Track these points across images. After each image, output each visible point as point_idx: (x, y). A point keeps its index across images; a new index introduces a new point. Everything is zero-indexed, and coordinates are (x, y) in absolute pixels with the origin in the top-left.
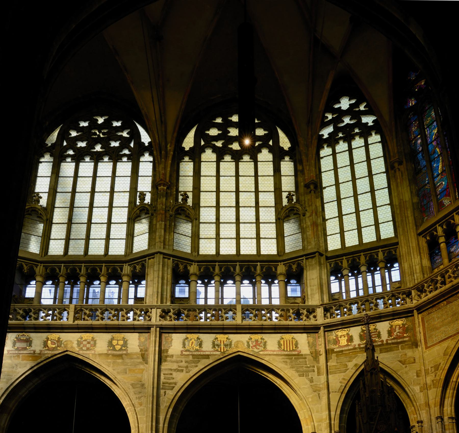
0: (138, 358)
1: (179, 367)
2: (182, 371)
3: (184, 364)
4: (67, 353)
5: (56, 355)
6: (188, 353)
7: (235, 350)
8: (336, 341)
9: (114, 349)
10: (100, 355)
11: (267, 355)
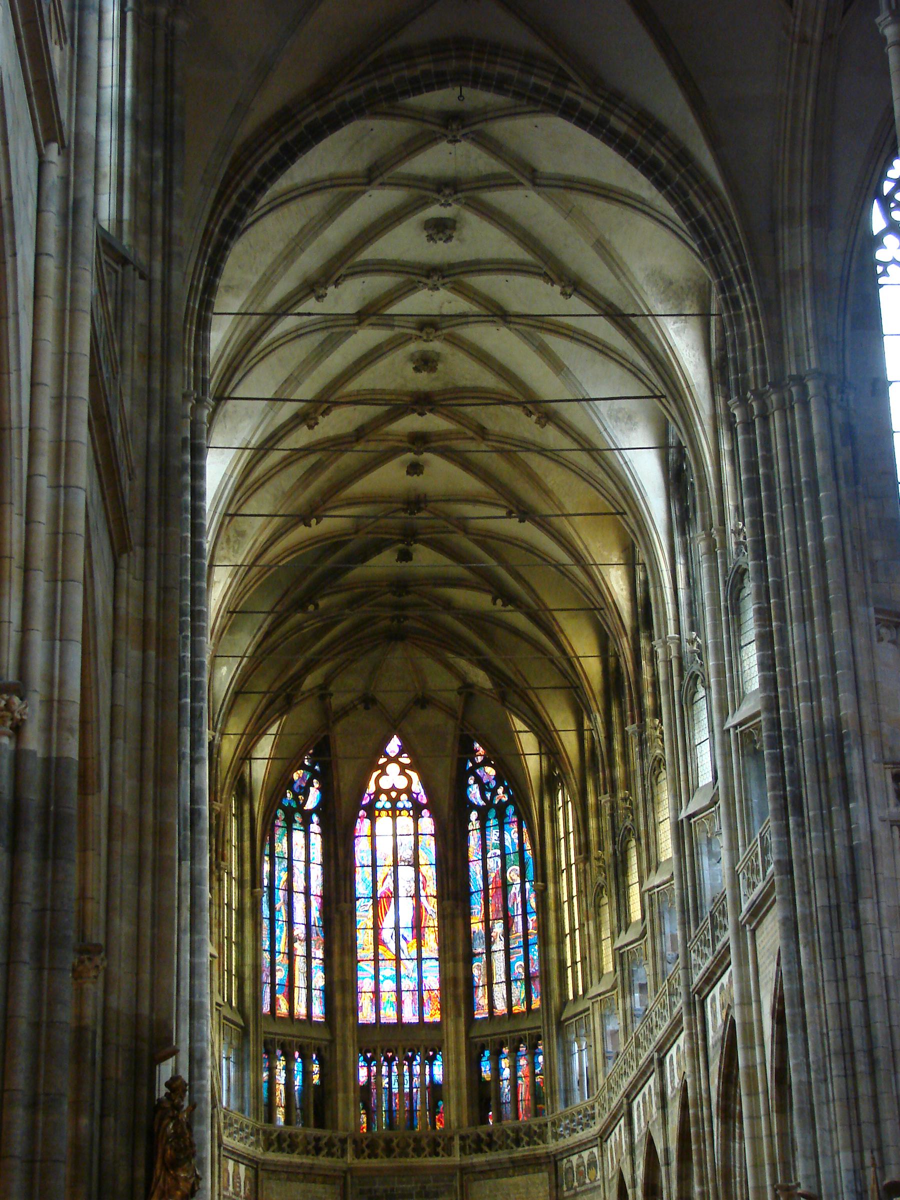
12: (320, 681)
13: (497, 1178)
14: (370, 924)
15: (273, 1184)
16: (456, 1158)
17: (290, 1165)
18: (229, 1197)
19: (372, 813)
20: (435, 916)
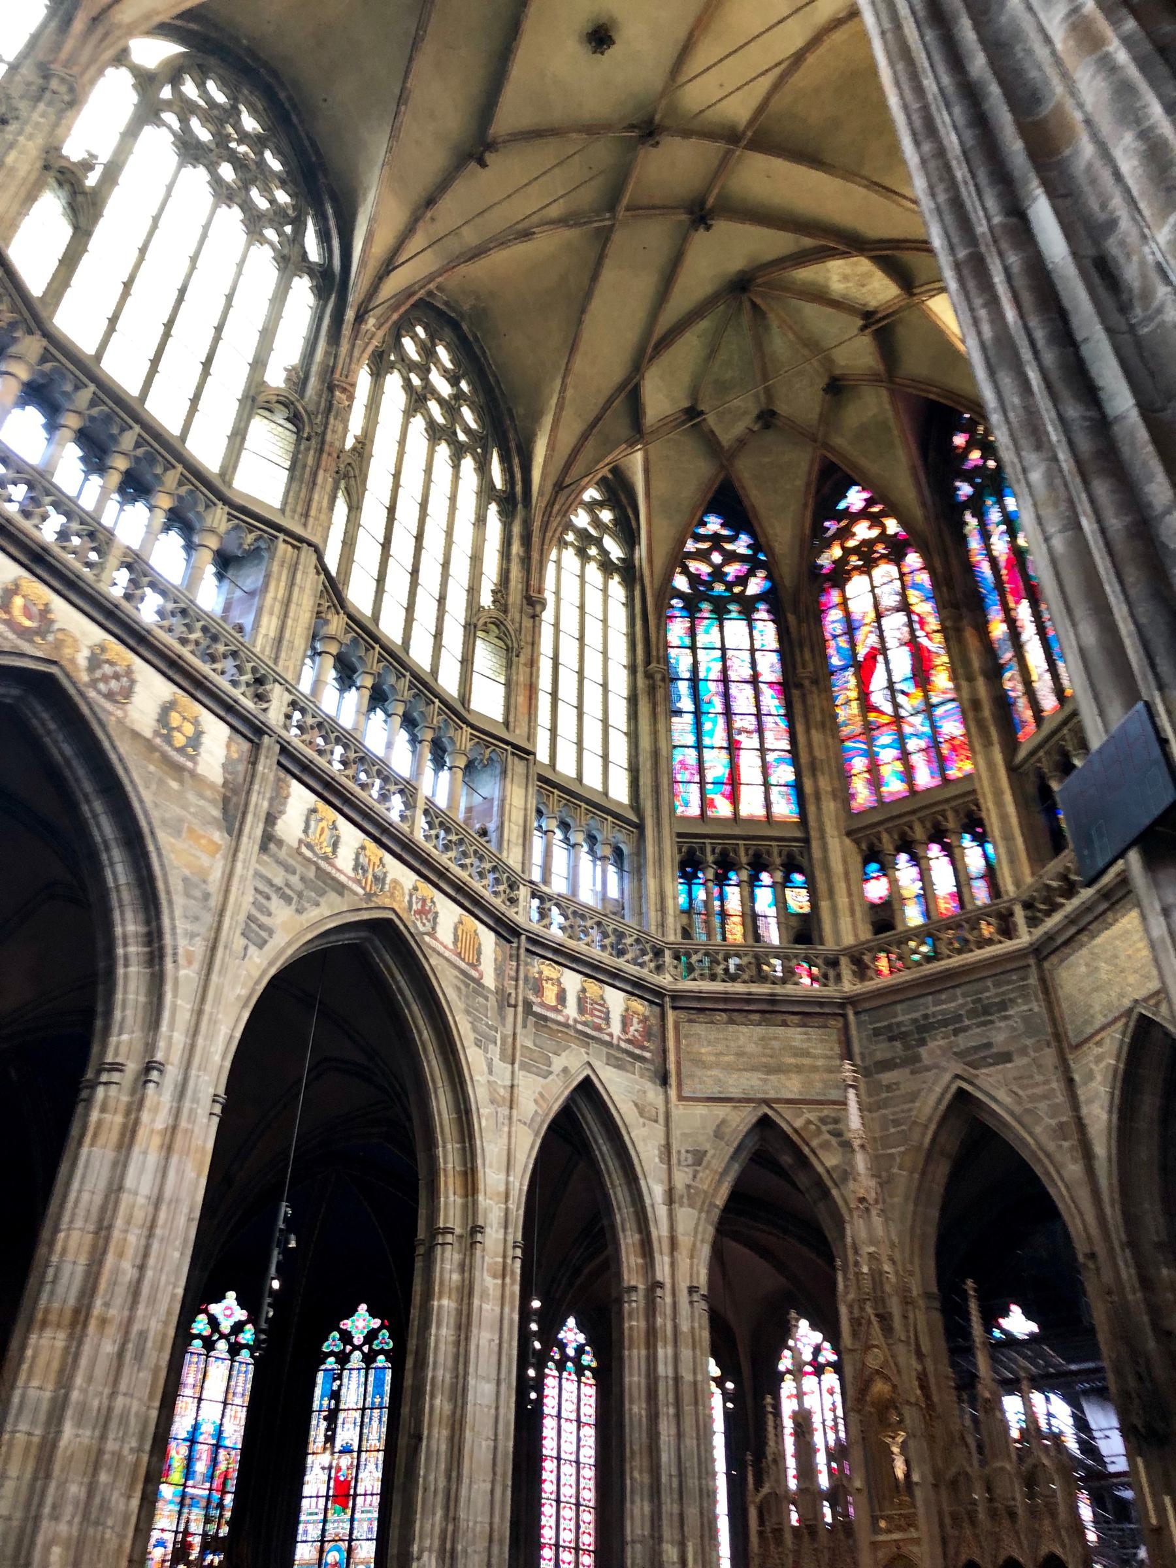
0: (213, 802)
1: (287, 885)
2: (288, 900)
3: (295, 880)
4: (53, 670)
5: (22, 655)
6: (308, 854)
7: (387, 902)
8: (539, 990)
9: (168, 739)
10: (136, 735)
11: (439, 954)
12: (686, 404)
13: (1093, 937)
14: (853, 694)
15: (700, 1029)
16: (1024, 938)
17: (726, 998)
18: (567, 1025)
19: (839, 576)
20: (942, 651)
